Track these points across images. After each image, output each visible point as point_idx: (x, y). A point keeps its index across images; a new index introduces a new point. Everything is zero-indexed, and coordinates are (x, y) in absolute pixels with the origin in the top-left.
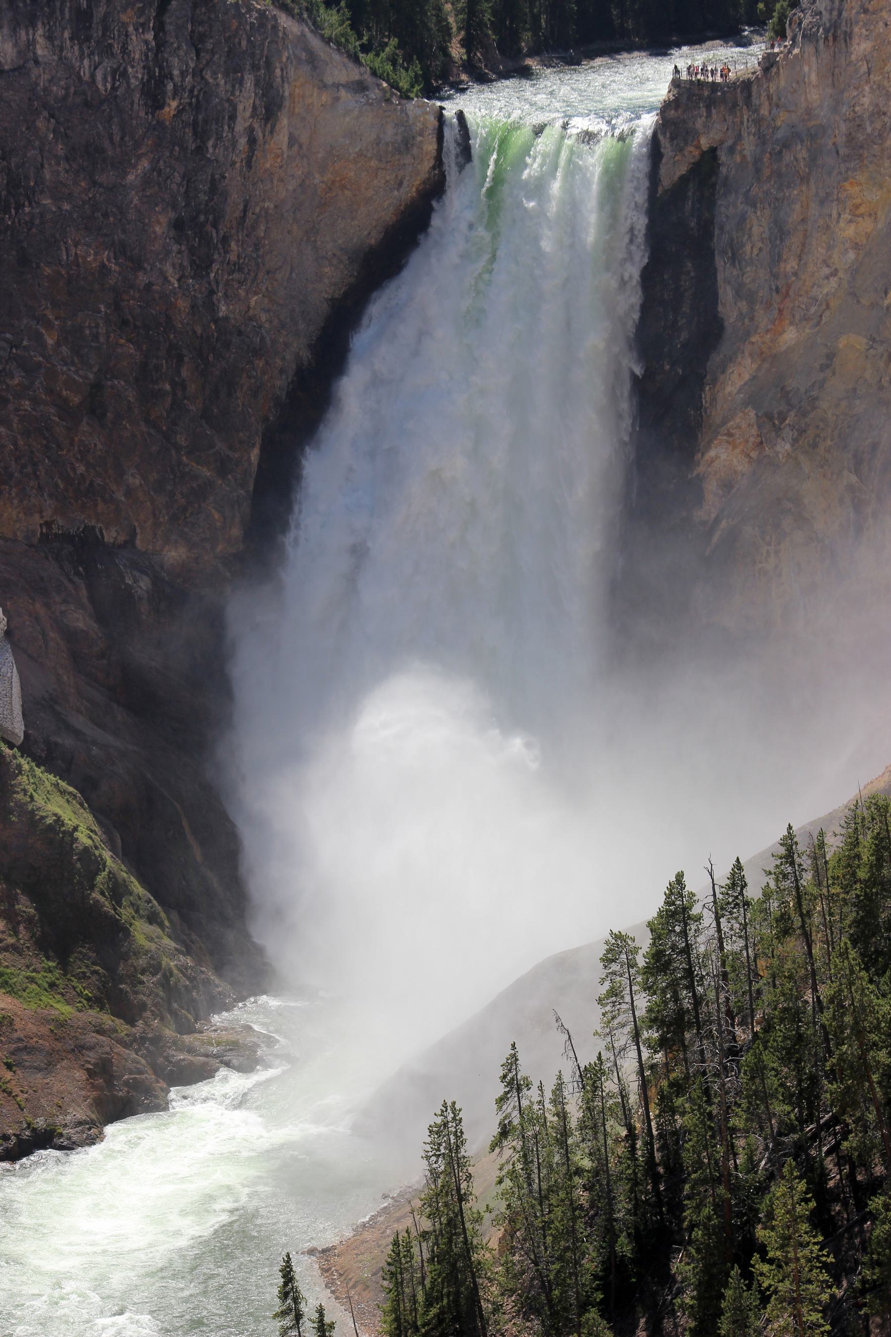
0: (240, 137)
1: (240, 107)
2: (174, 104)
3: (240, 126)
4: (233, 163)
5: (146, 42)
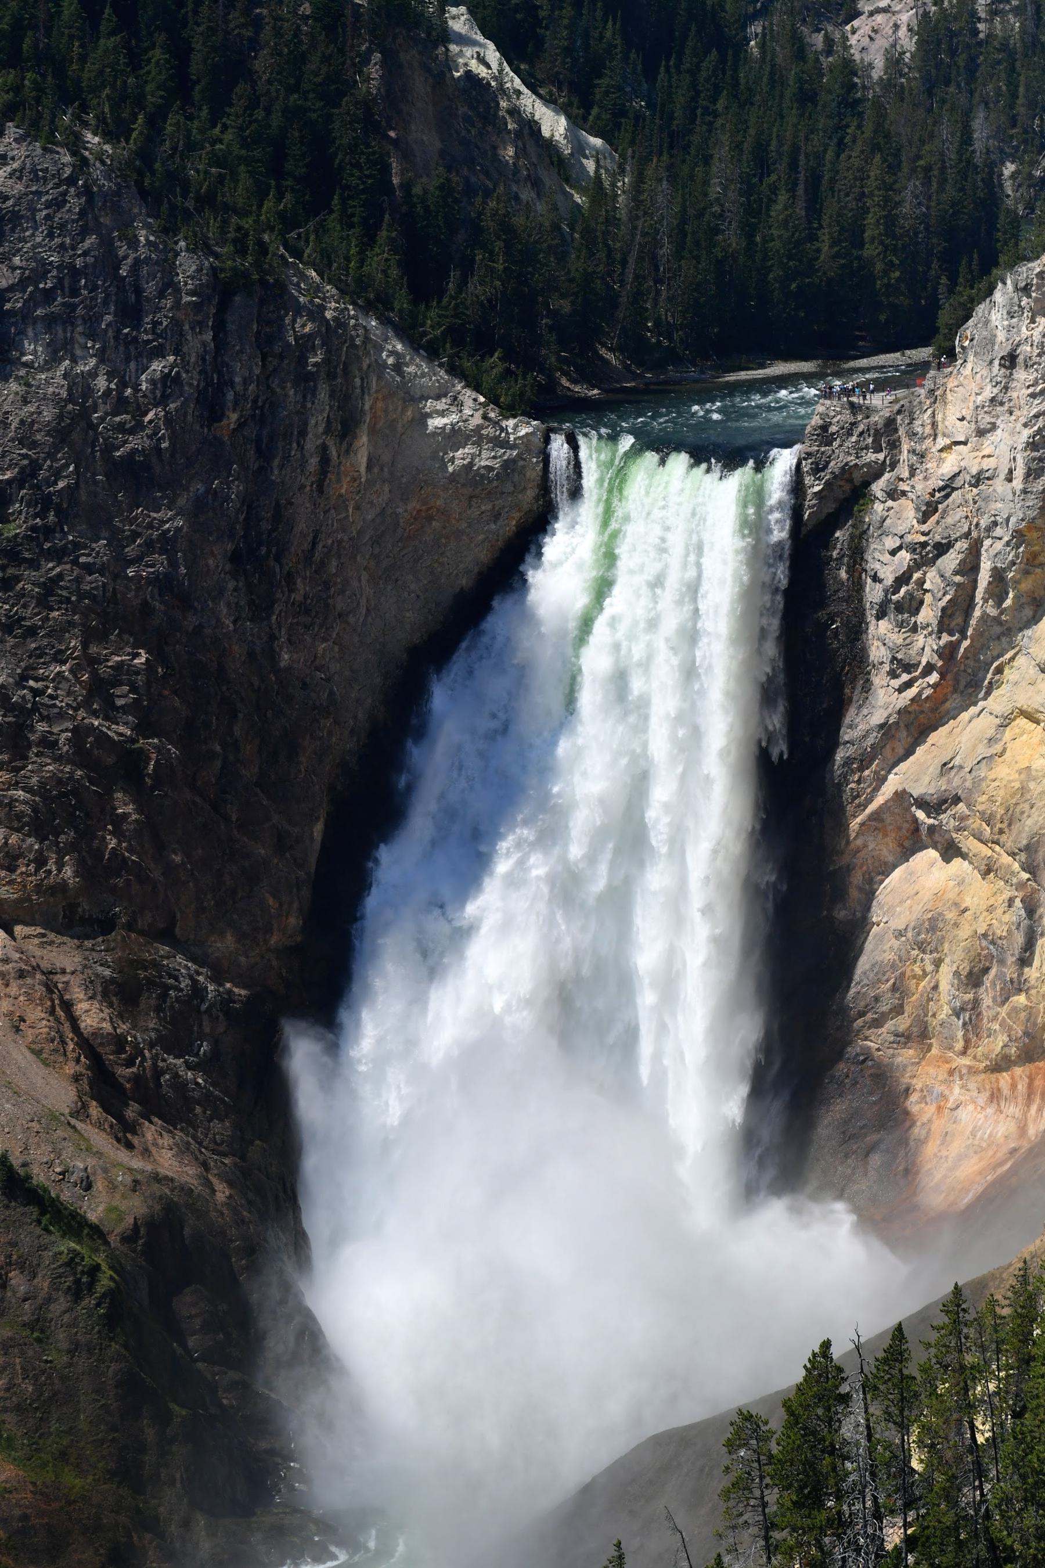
0: (311, 456)
1: (313, 422)
2: (234, 417)
3: (311, 444)
4: (302, 487)
5: (204, 344)
